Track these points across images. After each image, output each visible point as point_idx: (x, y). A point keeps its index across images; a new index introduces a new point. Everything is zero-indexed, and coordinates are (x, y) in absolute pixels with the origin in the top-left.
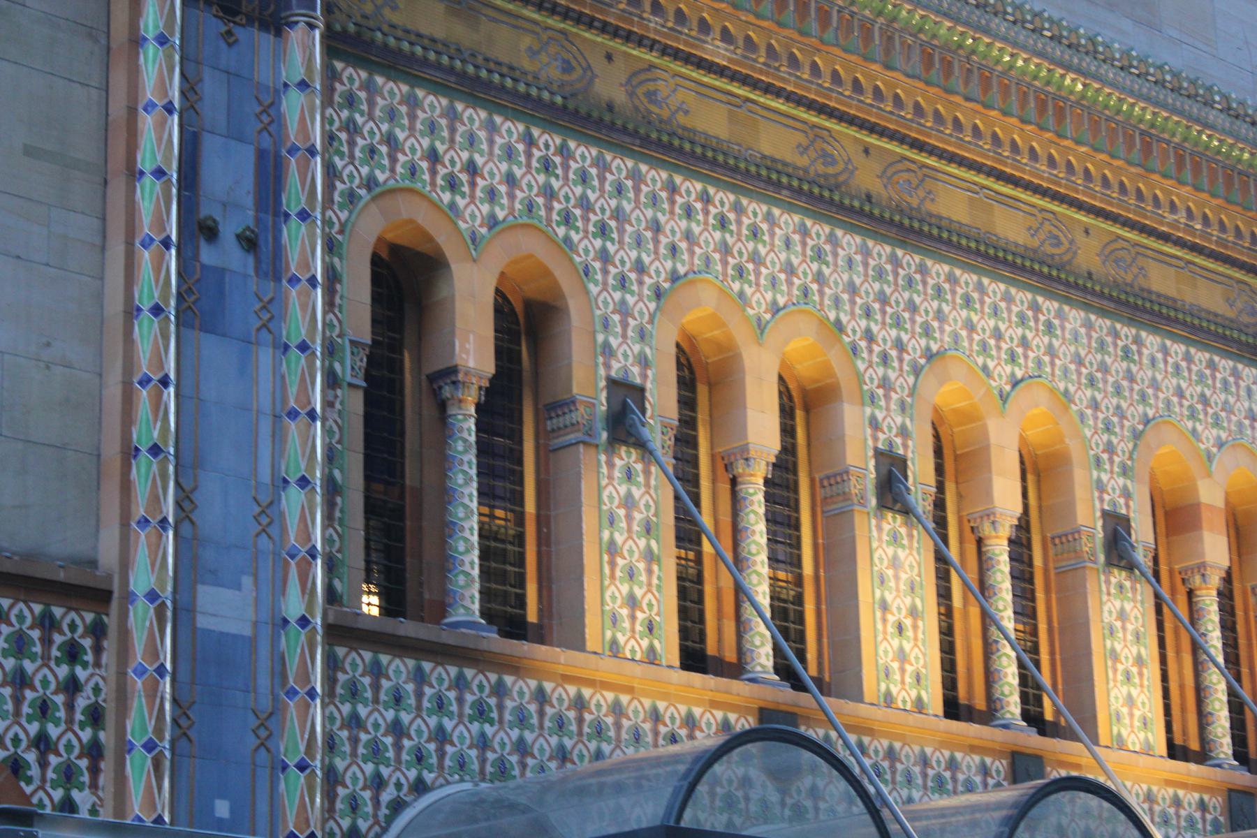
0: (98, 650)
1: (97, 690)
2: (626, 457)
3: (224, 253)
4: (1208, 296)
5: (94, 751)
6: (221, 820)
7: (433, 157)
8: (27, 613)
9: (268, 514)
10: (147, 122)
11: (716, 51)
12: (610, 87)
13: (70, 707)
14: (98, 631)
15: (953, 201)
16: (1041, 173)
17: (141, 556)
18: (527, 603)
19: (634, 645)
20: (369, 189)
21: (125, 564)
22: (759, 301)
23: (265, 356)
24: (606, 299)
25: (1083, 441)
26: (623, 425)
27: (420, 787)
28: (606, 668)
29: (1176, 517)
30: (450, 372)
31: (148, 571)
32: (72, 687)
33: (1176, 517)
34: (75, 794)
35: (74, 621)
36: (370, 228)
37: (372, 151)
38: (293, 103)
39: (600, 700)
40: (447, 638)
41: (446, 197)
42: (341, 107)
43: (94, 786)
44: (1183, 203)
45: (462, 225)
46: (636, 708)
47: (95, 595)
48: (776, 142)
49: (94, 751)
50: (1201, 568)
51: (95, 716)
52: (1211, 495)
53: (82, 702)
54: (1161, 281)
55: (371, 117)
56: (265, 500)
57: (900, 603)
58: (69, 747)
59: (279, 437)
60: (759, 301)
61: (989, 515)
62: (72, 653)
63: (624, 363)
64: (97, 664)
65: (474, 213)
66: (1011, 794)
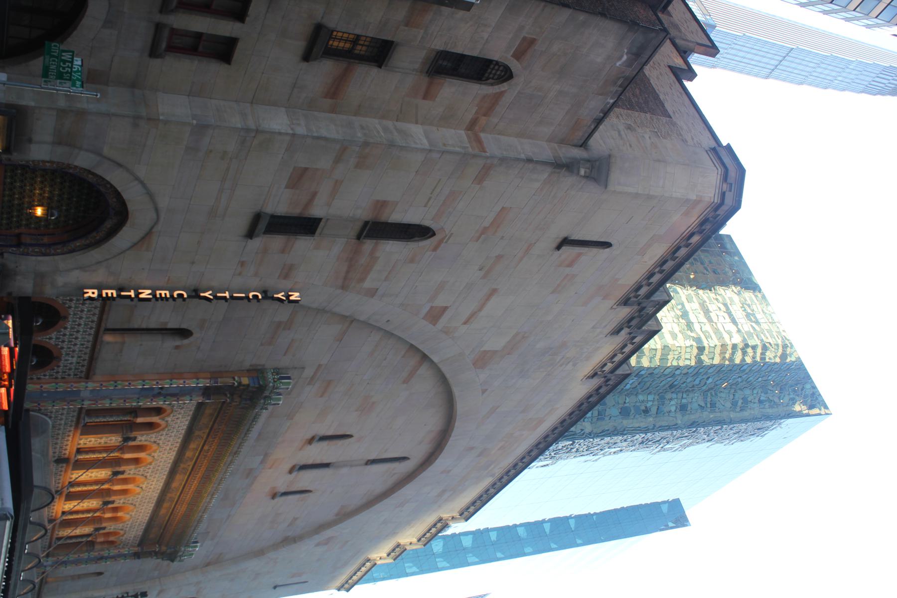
2: (120, 439)
3: (156, 392)
4: (163, 511)
5: (56, 378)
9: (104, 398)
10: (182, 381)
11: (206, 448)
12: (197, 433)
14: (81, 378)
15: (179, 479)
16: (186, 489)
17: (95, 385)
18: (88, 430)
19: (81, 442)
21: (94, 382)
22: (156, 455)
23: (137, 396)
24: (154, 436)
25: (130, 498)
26: (126, 439)
27: (50, 417)
28: (77, 439)
29: (116, 510)
30: (136, 417)
31: (91, 385)
32: (69, 375)
33: (116, 510)
35: (83, 375)
36: (164, 406)
38: (188, 397)
39: (70, 438)
40: (83, 415)
44: (182, 509)
46: (69, 443)
47: (88, 377)
48: (189, 454)
49: (56, 378)
50: (104, 513)
52: (120, 514)
54: (166, 505)
57: (93, 475)
59: (120, 399)
60: (156, 455)
61: (113, 485)
63: (139, 438)
65: (169, 419)
66: (53, 491)
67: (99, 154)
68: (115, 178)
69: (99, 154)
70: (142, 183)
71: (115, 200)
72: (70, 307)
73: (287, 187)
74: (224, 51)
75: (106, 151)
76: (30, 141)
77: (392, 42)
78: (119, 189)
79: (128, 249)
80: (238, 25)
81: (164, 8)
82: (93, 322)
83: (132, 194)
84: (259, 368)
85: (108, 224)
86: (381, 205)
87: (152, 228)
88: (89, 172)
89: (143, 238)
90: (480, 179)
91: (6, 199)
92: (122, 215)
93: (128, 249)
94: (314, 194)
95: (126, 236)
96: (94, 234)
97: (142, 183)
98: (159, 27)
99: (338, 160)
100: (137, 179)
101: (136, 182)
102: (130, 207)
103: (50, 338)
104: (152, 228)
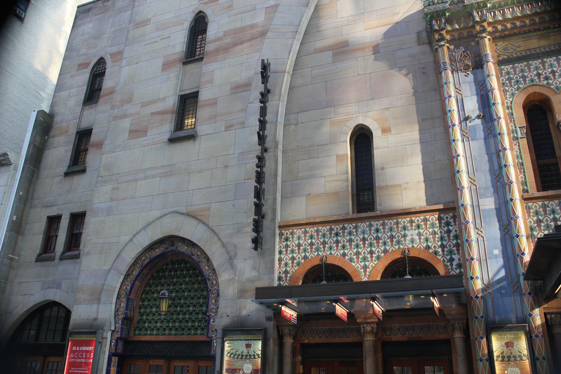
0: (455, 222)
1: (456, 231)
6: (496, 255)
7: (539, 75)
8: (434, 218)
13: (449, 236)
20: (518, 90)
34: (453, 256)
36: (520, 99)
37: (517, 82)
41: (545, 82)
42: (505, 76)
43: (458, 253)
45: (552, 87)
51: (456, 237)
53: (452, 235)
55: (515, 74)
56: (497, 173)
58: (450, 245)
62: (448, 224)
64: (455, 225)
67: (110, 270)
68: (130, 255)
69: (110, 270)
70: (135, 235)
71: (157, 250)
72: (305, 258)
73: (146, 135)
74: (78, 219)
75: (107, 267)
76: (96, 319)
77: (77, 133)
78: (140, 249)
79: (207, 225)
80: (63, 217)
81: (52, 259)
82: (331, 229)
83: (145, 240)
84: (424, 35)
85: (183, 248)
86: (166, 66)
87: (183, 214)
88: (127, 275)
89: (194, 217)
90: (146, 22)
91: (173, 332)
92: (171, 240)
93: (207, 225)
94: (153, 114)
95: (190, 231)
96: (194, 257)
97: (135, 235)
98: (62, 259)
99: (125, 116)
100: (131, 240)
101: (135, 240)
102: (159, 236)
103: (365, 267)
104: (183, 214)
